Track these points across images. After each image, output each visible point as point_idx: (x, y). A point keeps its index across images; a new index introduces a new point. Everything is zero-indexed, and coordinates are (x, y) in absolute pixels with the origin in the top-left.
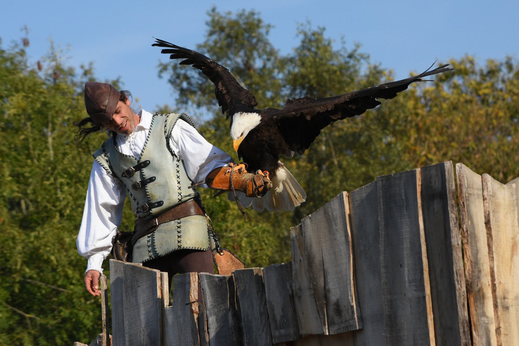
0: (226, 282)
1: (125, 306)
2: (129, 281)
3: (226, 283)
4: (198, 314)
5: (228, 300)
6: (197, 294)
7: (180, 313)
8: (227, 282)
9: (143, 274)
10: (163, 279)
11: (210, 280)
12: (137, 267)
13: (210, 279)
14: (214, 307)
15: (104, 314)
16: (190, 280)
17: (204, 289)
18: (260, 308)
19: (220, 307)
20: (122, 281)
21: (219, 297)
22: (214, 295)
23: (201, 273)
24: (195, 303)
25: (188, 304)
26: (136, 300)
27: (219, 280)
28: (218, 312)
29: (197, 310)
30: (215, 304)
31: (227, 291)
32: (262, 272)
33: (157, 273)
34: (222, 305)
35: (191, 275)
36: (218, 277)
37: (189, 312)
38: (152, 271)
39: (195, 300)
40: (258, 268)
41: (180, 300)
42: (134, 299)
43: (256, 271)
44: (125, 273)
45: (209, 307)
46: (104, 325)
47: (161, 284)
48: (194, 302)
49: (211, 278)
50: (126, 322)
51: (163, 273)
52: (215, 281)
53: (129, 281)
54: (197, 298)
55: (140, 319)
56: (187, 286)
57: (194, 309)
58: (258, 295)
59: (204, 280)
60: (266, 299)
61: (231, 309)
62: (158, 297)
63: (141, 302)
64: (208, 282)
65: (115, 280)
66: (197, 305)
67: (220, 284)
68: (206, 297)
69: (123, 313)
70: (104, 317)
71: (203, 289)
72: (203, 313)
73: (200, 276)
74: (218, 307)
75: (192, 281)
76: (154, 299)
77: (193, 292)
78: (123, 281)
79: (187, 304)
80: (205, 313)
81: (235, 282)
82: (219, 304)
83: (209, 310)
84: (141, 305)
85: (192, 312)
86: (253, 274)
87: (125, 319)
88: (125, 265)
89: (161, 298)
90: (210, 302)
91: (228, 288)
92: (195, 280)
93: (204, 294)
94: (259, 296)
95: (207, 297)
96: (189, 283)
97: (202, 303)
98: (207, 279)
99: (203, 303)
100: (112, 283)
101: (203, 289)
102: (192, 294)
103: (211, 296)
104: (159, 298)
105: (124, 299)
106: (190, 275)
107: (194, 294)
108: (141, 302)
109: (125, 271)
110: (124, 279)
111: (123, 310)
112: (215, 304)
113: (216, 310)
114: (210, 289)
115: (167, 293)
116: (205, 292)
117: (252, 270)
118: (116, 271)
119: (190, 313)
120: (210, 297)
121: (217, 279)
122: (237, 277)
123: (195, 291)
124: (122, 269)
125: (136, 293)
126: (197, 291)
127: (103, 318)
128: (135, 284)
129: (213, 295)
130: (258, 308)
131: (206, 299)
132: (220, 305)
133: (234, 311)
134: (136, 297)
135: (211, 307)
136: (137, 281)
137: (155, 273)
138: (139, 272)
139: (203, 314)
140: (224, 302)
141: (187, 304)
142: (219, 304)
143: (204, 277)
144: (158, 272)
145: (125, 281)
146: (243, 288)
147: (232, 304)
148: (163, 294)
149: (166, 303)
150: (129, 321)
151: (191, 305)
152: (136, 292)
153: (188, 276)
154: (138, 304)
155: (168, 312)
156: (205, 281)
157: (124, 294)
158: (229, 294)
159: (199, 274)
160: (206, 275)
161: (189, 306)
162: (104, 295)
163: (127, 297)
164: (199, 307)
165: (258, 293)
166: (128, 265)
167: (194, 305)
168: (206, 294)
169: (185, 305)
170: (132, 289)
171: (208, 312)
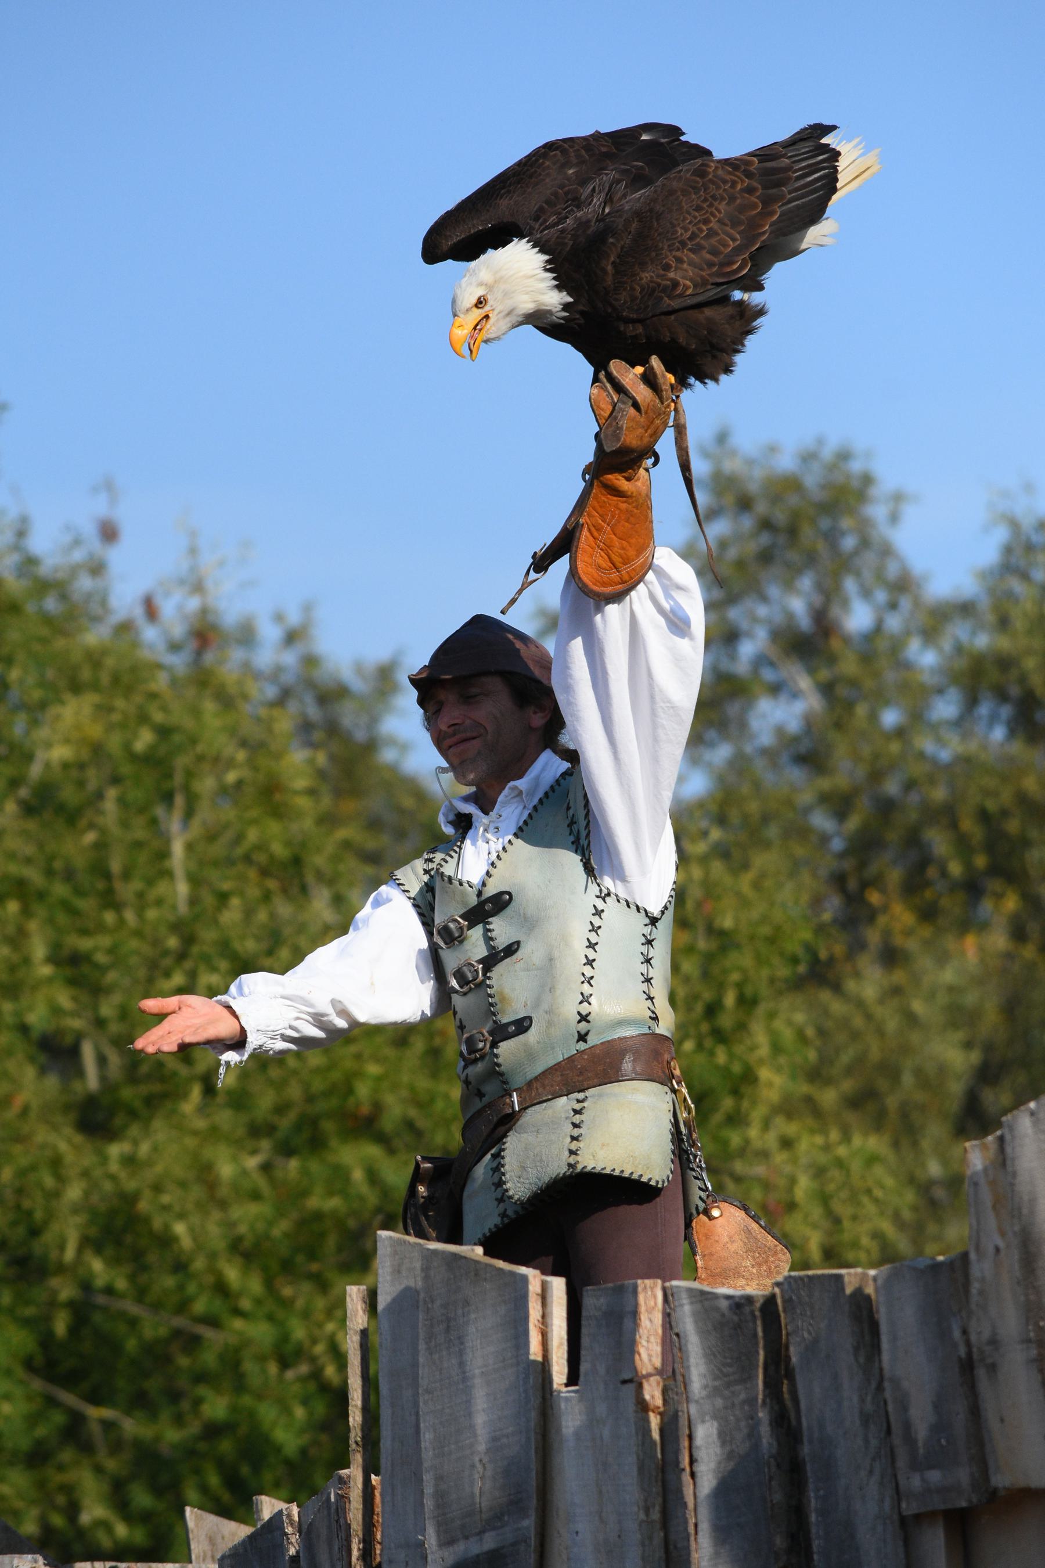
0: (752, 1313)
1: (424, 1383)
2: (438, 1303)
3: (754, 1317)
4: (661, 1414)
5: (761, 1371)
6: (659, 1349)
7: (601, 1409)
8: (757, 1313)
9: (485, 1280)
10: (549, 1300)
11: (703, 1306)
12: (465, 1258)
13: (701, 1301)
14: (715, 1392)
15: (356, 1406)
16: (636, 1305)
17: (682, 1335)
18: (862, 1401)
19: (733, 1393)
20: (418, 1302)
21: (729, 1361)
22: (715, 1356)
23: (675, 1283)
24: (652, 1379)
25: (630, 1381)
26: (461, 1364)
27: (730, 1308)
28: (726, 1408)
29: (659, 1402)
30: (717, 1383)
31: (757, 1344)
32: (871, 1282)
33: (531, 1279)
34: (738, 1388)
35: (640, 1289)
36: (728, 1297)
37: (631, 1407)
38: (512, 1274)
39: (650, 1370)
40: (859, 1270)
41: (602, 1369)
42: (454, 1361)
43: (853, 1280)
44: (426, 1278)
45: (696, 1391)
46: (356, 1443)
47: (544, 1316)
48: (649, 1376)
49: (706, 1299)
50: (427, 1436)
51: (549, 1278)
52: (717, 1309)
53: (438, 1303)
54: (658, 1362)
55: (472, 1427)
56: (627, 1323)
57: (647, 1397)
58: (857, 1360)
59: (682, 1305)
60: (881, 1369)
61: (768, 1400)
62: (532, 1357)
63: (477, 1371)
64: (695, 1314)
65: (394, 1300)
66: (658, 1383)
67: (736, 1318)
68: (688, 1360)
69: (416, 1404)
70: (355, 1418)
71: (677, 1335)
72: (676, 1412)
73: (669, 1292)
74: (727, 1393)
75: (642, 1309)
76: (518, 1364)
77: (644, 1343)
78: (421, 1303)
79: (624, 1382)
80: (683, 1411)
81: (782, 1315)
82: (728, 1385)
83: (697, 1402)
84: (478, 1381)
85: (643, 1407)
86: (843, 1289)
87: (422, 1425)
88: (428, 1250)
89: (540, 1359)
90: (699, 1375)
91: (760, 1333)
92: (652, 1303)
93: (680, 1349)
94: (862, 1360)
95: (693, 1361)
96: (635, 1314)
97: (675, 1380)
98: (692, 1303)
99: (679, 1378)
100: (384, 1309)
101: (677, 1335)
102: (642, 1351)
103: (706, 1355)
104: (535, 1362)
105: (421, 1360)
106: (635, 1288)
107: (648, 1349)
108: (477, 1371)
109: (426, 1269)
110: (422, 1295)
111: (416, 1395)
112: (717, 1383)
113: (719, 1402)
114: (702, 1333)
115: (561, 1344)
116: (686, 1345)
117: (839, 1278)
118: (397, 1271)
119: (636, 1412)
120: (702, 1361)
121: (724, 1304)
122: (791, 1298)
123: (652, 1339)
124: (418, 1265)
125: (462, 1343)
126: (659, 1341)
127: (351, 1419)
128: (460, 1312)
129: (710, 1355)
130: (856, 1399)
131: (688, 1367)
132: (732, 1389)
133: (776, 1408)
134: (461, 1353)
135: (704, 1393)
136: (467, 1303)
137: (525, 1279)
138: (473, 1274)
139: (676, 1416)
140: (746, 1376)
141: (624, 1382)
142: (728, 1385)
143: (684, 1295)
144: (535, 1277)
145: (425, 1302)
146: (810, 1333)
147: (772, 1386)
148: (550, 1347)
149: (559, 1373)
150: (435, 1431)
151: (640, 1386)
152: (461, 1339)
153: (631, 1289)
154: (465, 1378)
155: (563, 1405)
156: (687, 1308)
157: (422, 1346)
158: (762, 1353)
159: (667, 1284)
160: (690, 1290)
161: (631, 1388)
162: (357, 1346)
163: (431, 1354)
164: (665, 1392)
165: (856, 1349)
166: (435, 1252)
167: (650, 1385)
168: (687, 1351)
169: (619, 1385)
170: (448, 1327)
171: (693, 1409)
